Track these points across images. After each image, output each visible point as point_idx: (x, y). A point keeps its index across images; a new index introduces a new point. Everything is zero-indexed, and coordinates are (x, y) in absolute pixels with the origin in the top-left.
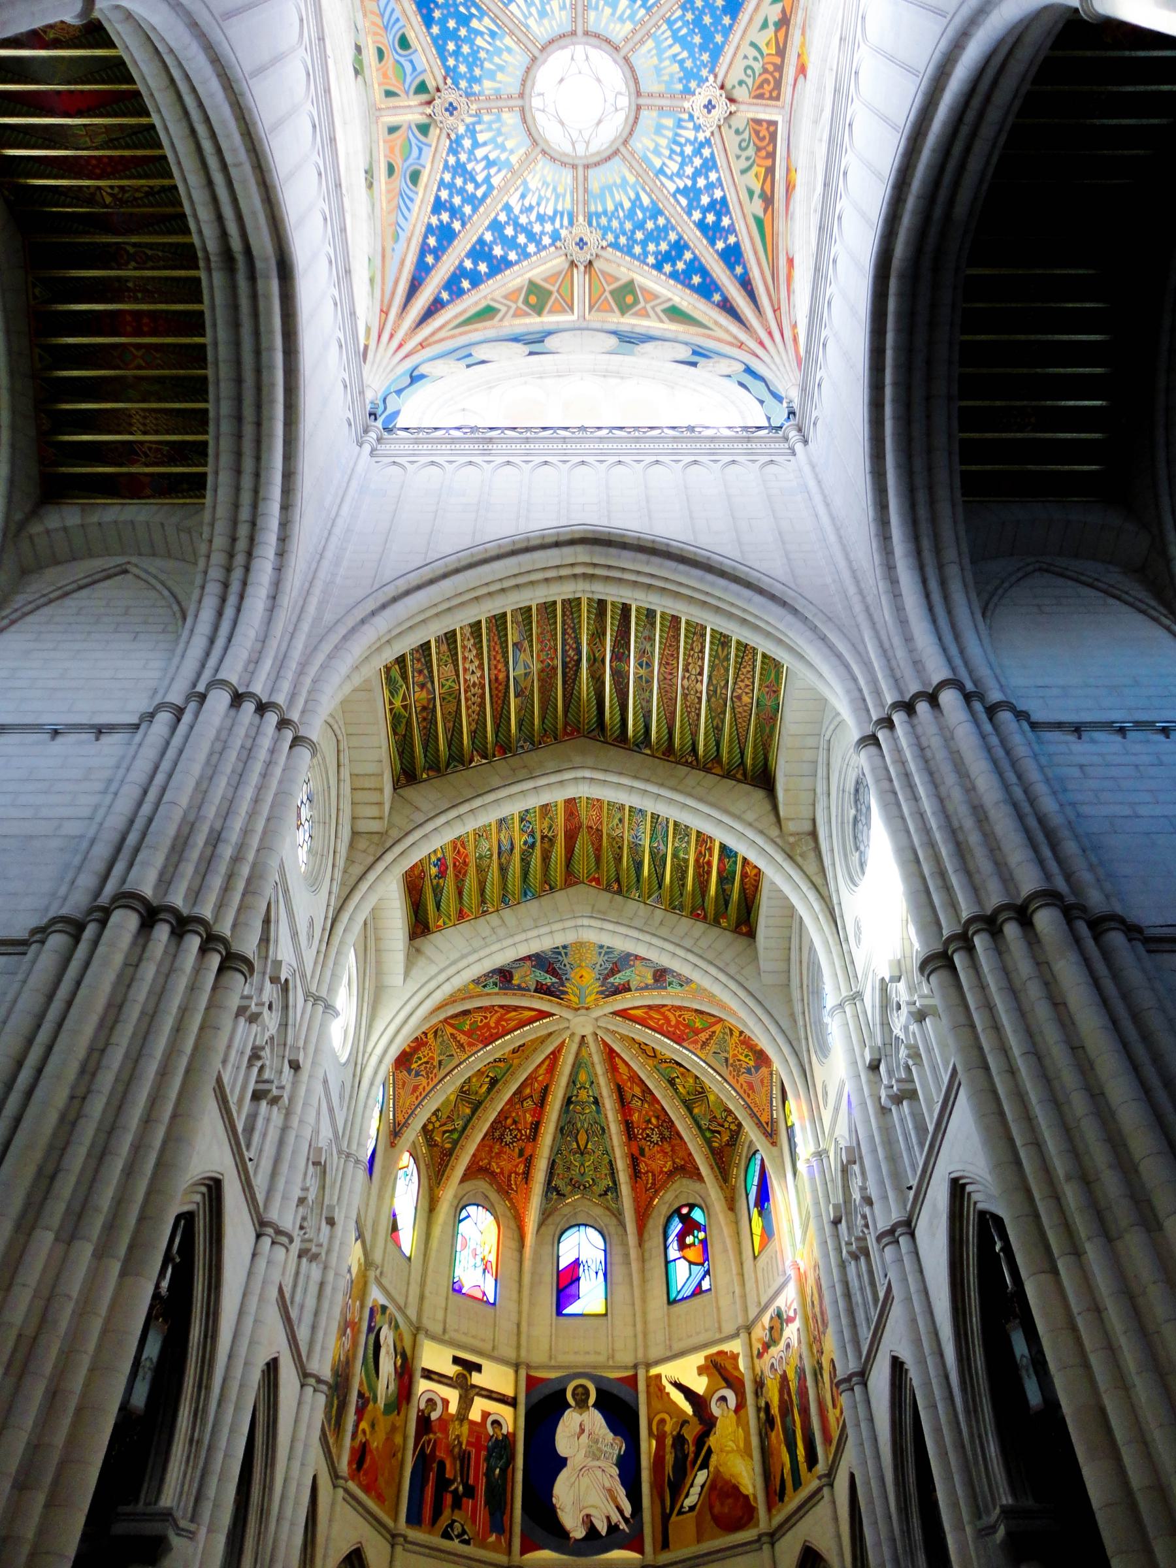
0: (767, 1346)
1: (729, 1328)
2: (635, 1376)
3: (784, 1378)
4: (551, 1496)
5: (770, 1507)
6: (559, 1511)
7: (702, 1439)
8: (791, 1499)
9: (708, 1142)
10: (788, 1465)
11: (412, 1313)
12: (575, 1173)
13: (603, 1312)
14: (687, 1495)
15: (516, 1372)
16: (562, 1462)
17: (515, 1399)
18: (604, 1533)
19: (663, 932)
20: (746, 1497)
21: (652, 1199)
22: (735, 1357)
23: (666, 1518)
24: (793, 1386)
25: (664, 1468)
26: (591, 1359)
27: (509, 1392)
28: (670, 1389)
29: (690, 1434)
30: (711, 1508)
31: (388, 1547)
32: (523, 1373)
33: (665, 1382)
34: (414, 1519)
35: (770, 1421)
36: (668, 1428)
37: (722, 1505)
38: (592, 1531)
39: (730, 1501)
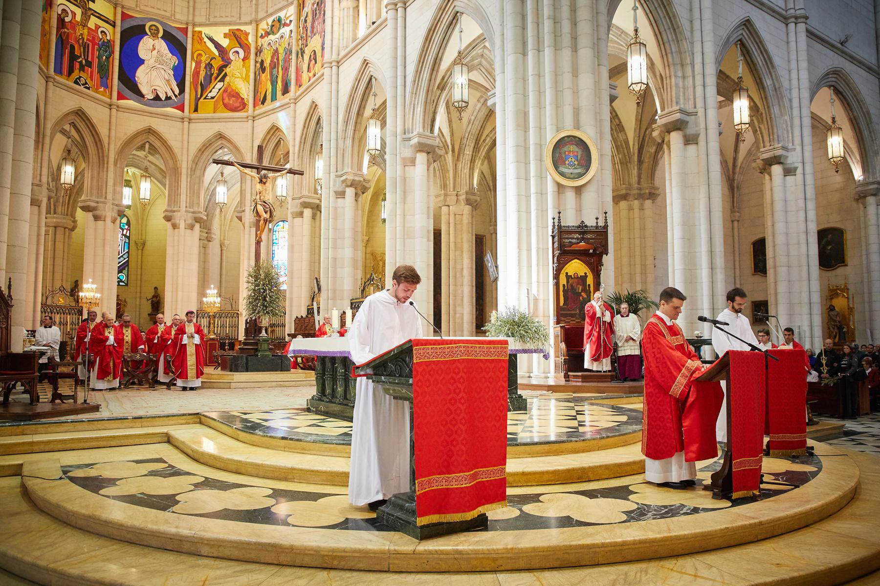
0: (268, 34)
1: (245, 18)
2: (187, 28)
3: (276, 51)
4: (135, 76)
6: (139, 85)
7: (221, 69)
8: (268, 105)
10: (269, 91)
14: (210, 92)
15: (115, 8)
16: (142, 62)
18: (163, 99)
20: (243, 99)
22: (247, 34)
24: (281, 57)
25: (198, 76)
26: (163, 13)
27: (111, 17)
28: (206, 40)
29: (217, 64)
30: (223, 100)
32: (119, 10)
33: (203, 36)
34: (58, 70)
35: (263, 70)
36: (203, 58)
37: (229, 99)
38: (157, 98)
39: (234, 99)
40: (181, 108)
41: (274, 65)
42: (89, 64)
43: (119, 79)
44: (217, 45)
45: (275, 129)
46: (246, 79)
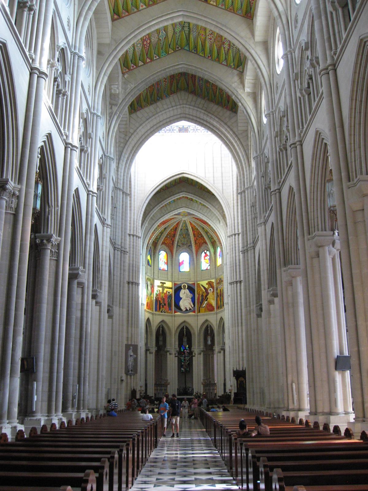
3: (221, 290)
5: (217, 309)
7: (206, 296)
9: (211, 240)
11: (152, 276)
12: (183, 242)
13: (188, 270)
16: (181, 298)
17: (172, 287)
19: (201, 211)
21: (199, 248)
23: (199, 308)
26: (186, 280)
27: (171, 286)
28: (201, 286)
29: (205, 295)
31: (152, 315)
34: (156, 310)
36: (201, 293)
38: (187, 310)
40: (194, 312)
41: (220, 295)
42: (165, 305)
43: (175, 306)
44: (204, 288)
45: (221, 319)
46: (214, 299)
